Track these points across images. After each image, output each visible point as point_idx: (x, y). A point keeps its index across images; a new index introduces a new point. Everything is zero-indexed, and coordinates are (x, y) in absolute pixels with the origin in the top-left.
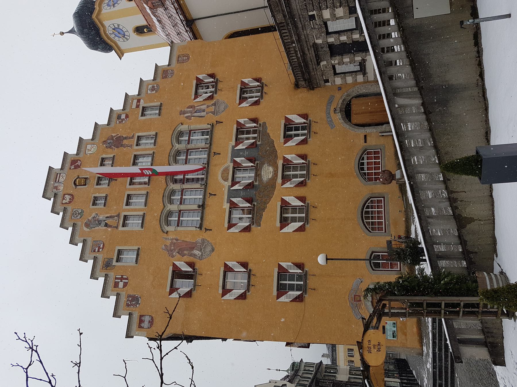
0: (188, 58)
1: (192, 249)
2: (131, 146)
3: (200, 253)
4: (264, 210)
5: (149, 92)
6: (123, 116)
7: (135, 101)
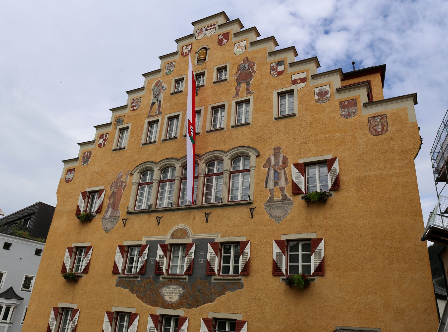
0: (378, 134)
1: (113, 208)
2: (237, 96)
3: (107, 217)
4: (132, 290)
5: (317, 90)
6: (280, 68)
7: (303, 75)
